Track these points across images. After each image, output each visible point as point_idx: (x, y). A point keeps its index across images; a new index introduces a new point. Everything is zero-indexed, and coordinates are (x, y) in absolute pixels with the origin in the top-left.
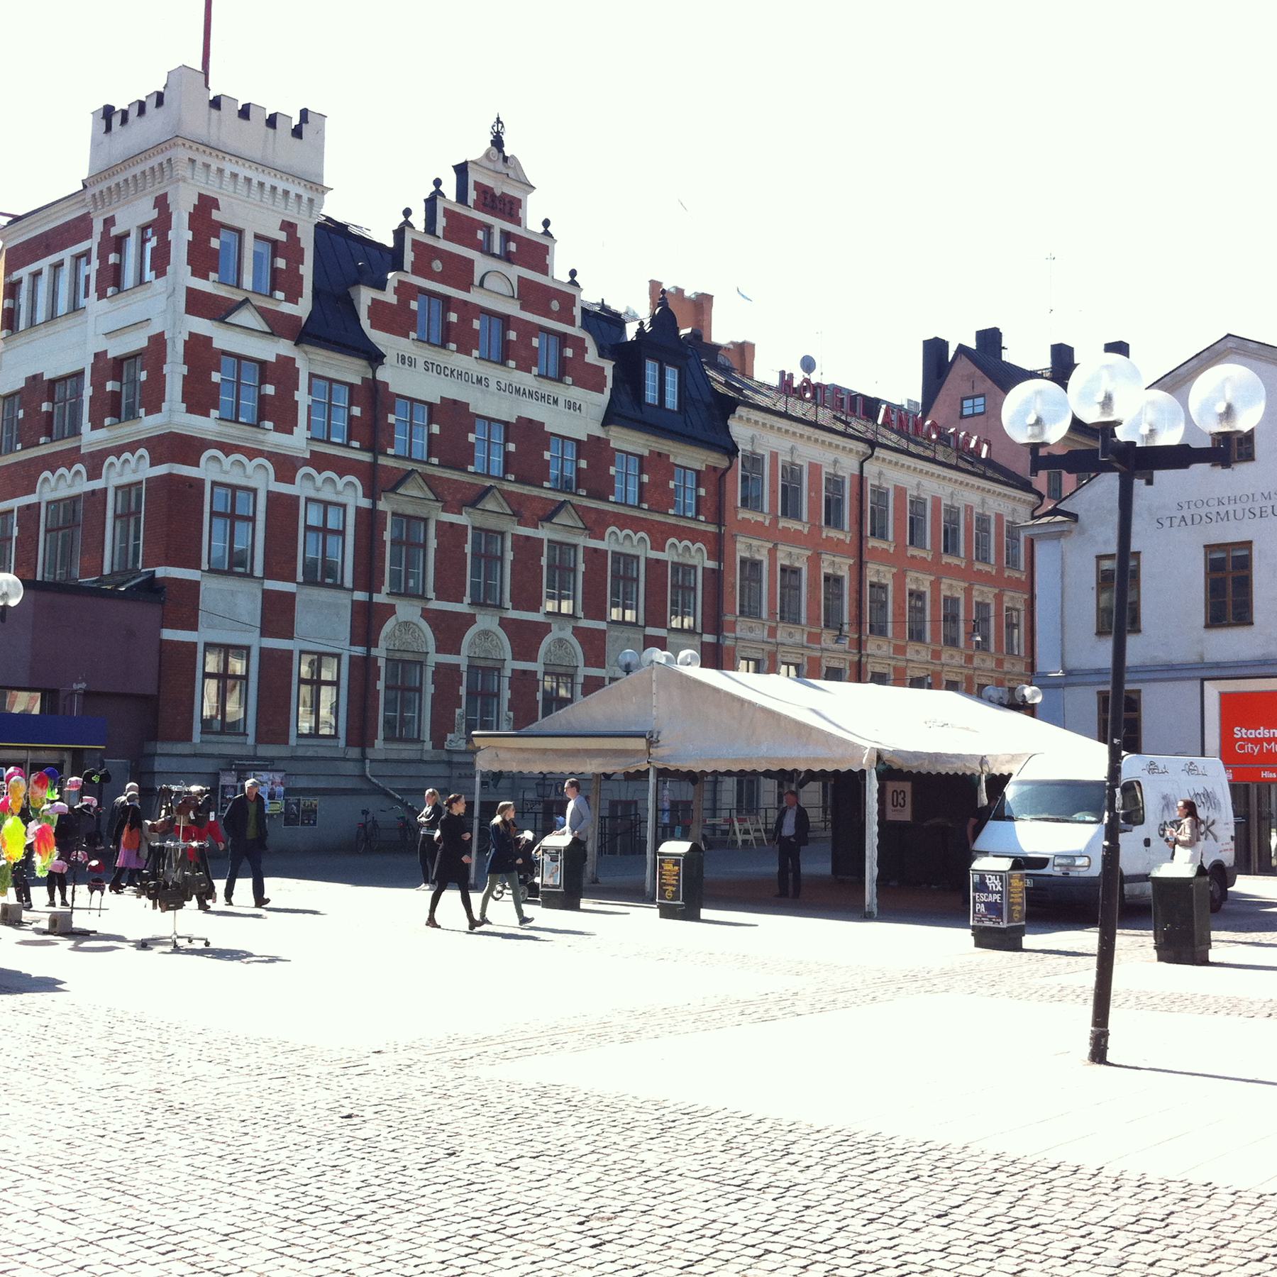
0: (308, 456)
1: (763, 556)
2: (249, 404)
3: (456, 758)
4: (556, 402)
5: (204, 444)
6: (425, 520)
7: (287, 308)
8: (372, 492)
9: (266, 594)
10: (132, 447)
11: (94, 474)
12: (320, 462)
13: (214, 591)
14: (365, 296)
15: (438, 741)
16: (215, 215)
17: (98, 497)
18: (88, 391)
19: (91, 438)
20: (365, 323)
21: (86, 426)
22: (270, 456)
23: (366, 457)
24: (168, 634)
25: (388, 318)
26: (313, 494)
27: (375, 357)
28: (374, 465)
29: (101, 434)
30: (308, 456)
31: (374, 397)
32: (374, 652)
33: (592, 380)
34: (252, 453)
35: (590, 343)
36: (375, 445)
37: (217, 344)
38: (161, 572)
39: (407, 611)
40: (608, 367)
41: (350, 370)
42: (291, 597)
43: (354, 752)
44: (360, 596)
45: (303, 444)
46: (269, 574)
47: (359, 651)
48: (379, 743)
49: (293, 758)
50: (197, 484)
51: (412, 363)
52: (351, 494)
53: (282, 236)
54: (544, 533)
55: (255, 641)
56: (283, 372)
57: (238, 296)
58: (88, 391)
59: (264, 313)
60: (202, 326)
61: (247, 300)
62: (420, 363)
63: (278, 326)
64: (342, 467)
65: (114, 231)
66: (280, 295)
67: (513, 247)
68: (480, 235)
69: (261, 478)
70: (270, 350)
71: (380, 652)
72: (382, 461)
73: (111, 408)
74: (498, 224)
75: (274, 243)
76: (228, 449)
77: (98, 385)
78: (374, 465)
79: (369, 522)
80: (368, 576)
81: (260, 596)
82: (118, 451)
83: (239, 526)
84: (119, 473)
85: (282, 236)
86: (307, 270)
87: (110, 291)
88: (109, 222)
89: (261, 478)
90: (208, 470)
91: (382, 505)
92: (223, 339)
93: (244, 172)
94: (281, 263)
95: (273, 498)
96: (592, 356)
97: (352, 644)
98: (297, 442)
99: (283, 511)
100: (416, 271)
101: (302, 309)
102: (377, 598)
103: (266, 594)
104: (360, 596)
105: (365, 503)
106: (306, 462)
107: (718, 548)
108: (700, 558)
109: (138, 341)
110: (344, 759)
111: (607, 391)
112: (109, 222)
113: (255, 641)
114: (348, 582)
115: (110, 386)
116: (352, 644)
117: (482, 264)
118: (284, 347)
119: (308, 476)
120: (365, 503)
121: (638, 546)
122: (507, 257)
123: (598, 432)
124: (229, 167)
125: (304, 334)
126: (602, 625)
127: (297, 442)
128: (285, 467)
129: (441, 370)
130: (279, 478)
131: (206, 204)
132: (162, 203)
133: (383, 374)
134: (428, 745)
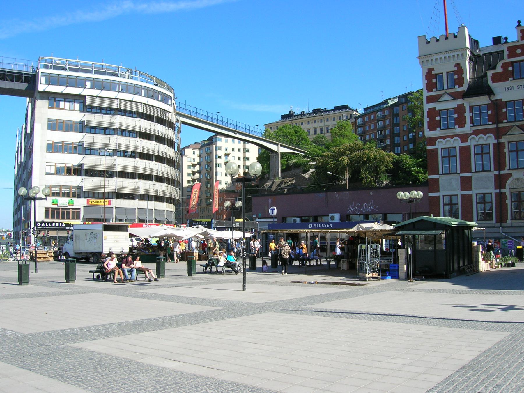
0: (472, 132)
7: (458, 89)
8: (498, 137)
9: (462, 178)
12: (476, 133)
13: (443, 180)
14: (490, 73)
16: (433, 72)
20: (490, 82)
22: (458, 136)
23: (494, 126)
25: (497, 78)
26: (476, 143)
27: (490, 92)
28: (498, 128)
30: (472, 132)
34: (452, 137)
36: (498, 121)
42: (471, 177)
44: (497, 172)
45: (469, 129)
46: (461, 172)
47: (498, 191)
48: (509, 221)
50: (436, 151)
51: (511, 88)
52: (491, 140)
53: (456, 69)
56: (460, 109)
57: (442, 92)
59: (450, 94)
60: (432, 105)
61: (446, 92)
62: (515, 87)
63: (455, 96)
64: (485, 132)
66: (457, 86)
70: (454, 104)
71: (506, 191)
72: (501, 125)
76: (444, 138)
78: (498, 128)
79: (499, 147)
80: (500, 164)
81: (459, 179)
83: (452, 159)
85: (456, 69)
89: (458, 143)
90: (439, 145)
91: (502, 141)
92: (438, 106)
94: (456, 77)
95: (461, 148)
97: (495, 189)
98: (467, 128)
99: (465, 151)
100: (509, 56)
101: (465, 88)
102: (502, 172)
104: (497, 172)
106: (471, 134)
113: (460, 193)
114: (492, 169)
116: (495, 189)
118: (460, 101)
119: (474, 138)
124: (434, 58)
127: (467, 128)
128: (464, 138)
133: (497, 97)
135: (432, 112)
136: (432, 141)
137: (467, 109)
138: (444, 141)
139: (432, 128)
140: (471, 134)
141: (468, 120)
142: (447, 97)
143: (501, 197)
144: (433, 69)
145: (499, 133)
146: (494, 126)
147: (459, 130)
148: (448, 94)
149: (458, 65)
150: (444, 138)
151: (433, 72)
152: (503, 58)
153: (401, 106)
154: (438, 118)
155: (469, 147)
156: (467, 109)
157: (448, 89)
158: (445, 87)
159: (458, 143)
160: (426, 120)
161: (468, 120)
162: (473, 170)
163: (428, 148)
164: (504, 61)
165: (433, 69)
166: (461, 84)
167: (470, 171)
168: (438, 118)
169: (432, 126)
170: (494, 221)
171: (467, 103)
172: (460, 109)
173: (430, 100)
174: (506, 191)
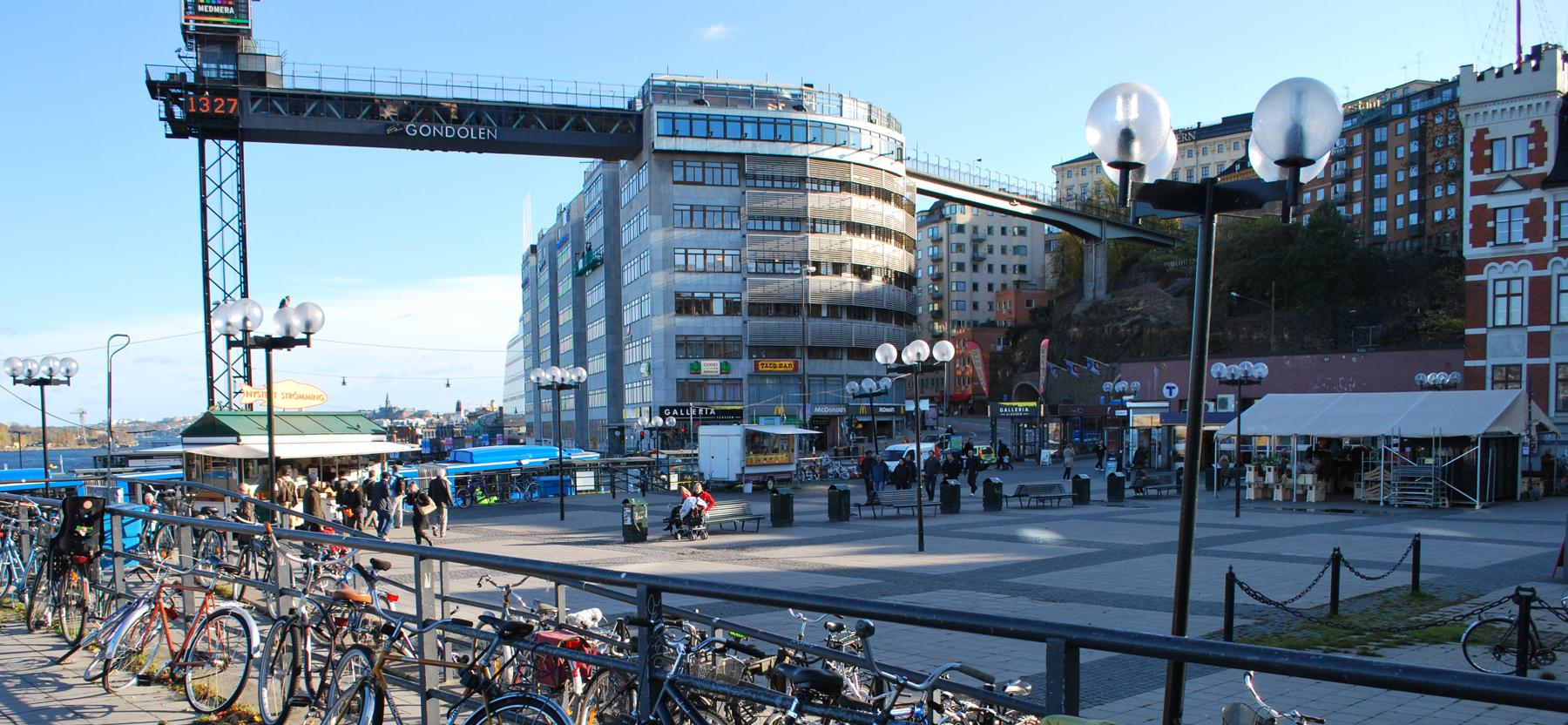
2: (1518, 234)
13: (1493, 338)
16: (1487, 137)
22: (1528, 257)
24: (1468, 363)
34: (1516, 259)
50: (1483, 284)
55: (1525, 361)
57: (1503, 176)
59: (1517, 180)
60: (1480, 200)
63: (1526, 183)
70: (1525, 199)
76: (1500, 260)
85: (1532, 131)
86: (1551, 145)
89: (1528, 271)
90: (1488, 275)
92: (1492, 202)
93: (1499, 107)
95: (1533, 281)
101: (1548, 167)
106: (1555, 255)
118: (1536, 193)
124: (1490, 109)
125: (1546, 182)
127: (1547, 244)
128: (1540, 261)
130: (1535, 268)
131: (1481, 133)
135: (1481, 213)
136: (1478, 266)
137: (1550, 208)
138: (1500, 267)
139: (1477, 242)
140: (1555, 255)
141: (1550, 228)
142: (1511, 185)
144: (1486, 131)
147: (1531, 247)
148: (1514, 179)
149: (1537, 124)
151: (1487, 137)
153: (1392, 124)
154: (1490, 224)
155: (1548, 279)
156: (1550, 208)
157: (1514, 169)
158: (1509, 167)
159: (1528, 271)
160: (1467, 226)
161: (1550, 228)
162: (1554, 321)
163: (1469, 278)
165: (1486, 131)
166: (1540, 163)
167: (1548, 323)
168: (1490, 224)
169: (1483, 236)
171: (1549, 198)
172: (1535, 211)
173: (1477, 189)
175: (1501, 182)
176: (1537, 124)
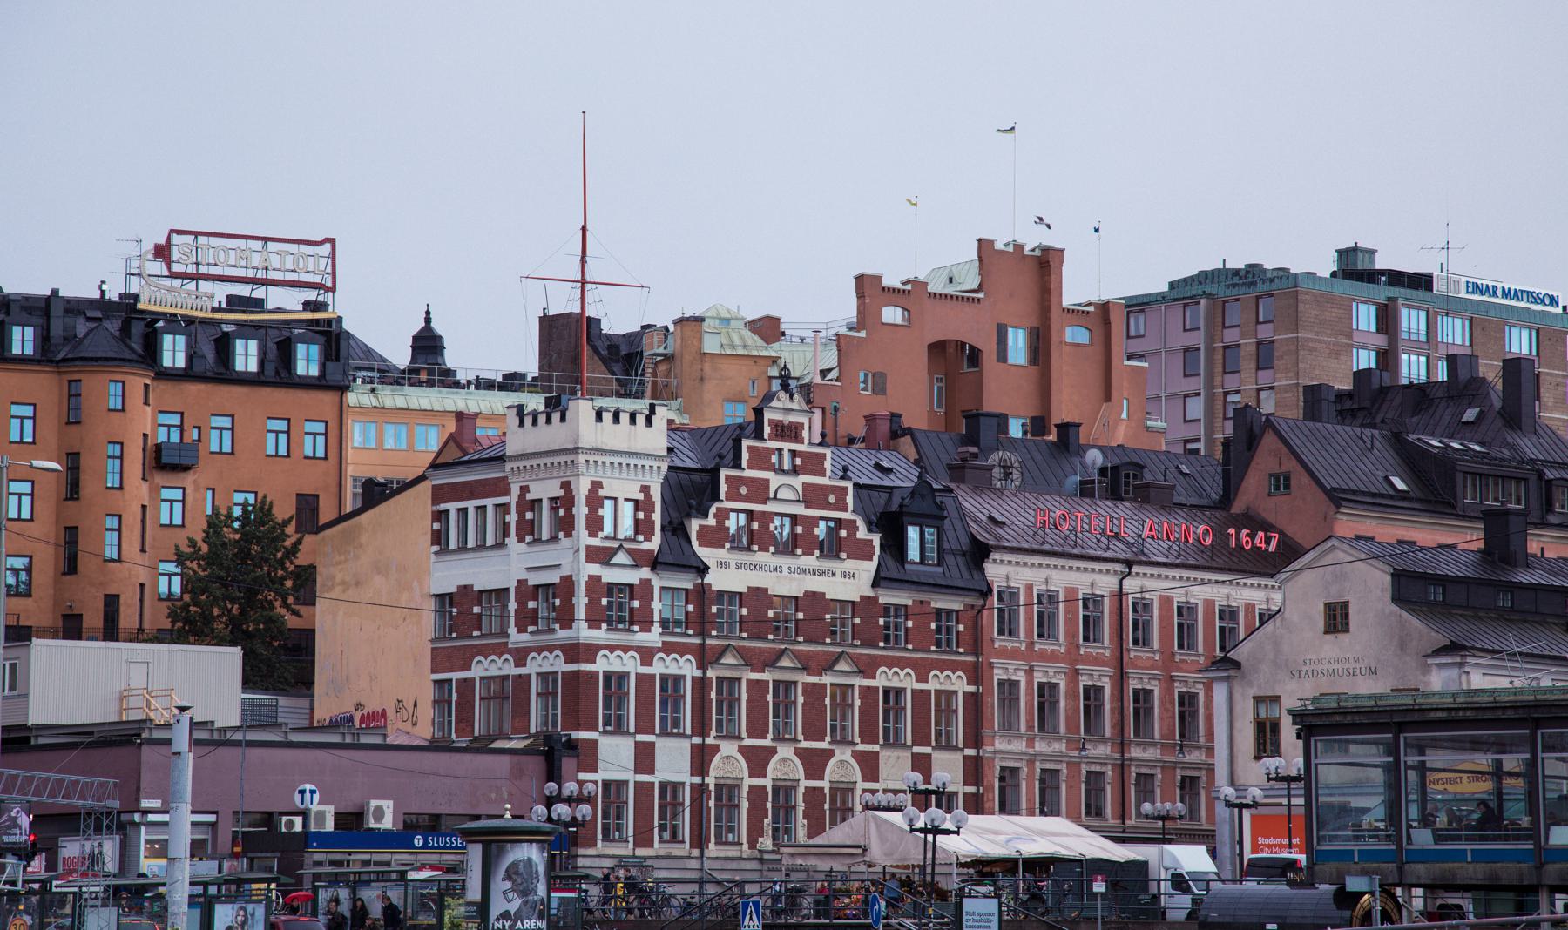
1: (1021, 677)
3: (766, 856)
4: (834, 574)
5: (599, 647)
6: (739, 680)
7: (646, 546)
8: (702, 665)
10: (551, 649)
11: (521, 662)
12: (668, 648)
14: (694, 525)
15: (752, 843)
17: (523, 681)
18: (512, 606)
19: (515, 638)
20: (695, 543)
21: (512, 630)
22: (638, 649)
27: (702, 570)
29: (525, 637)
31: (701, 594)
32: (707, 780)
33: (863, 552)
34: (626, 649)
35: (860, 523)
37: (605, 580)
38: (576, 735)
39: (729, 748)
40: (876, 539)
41: (686, 582)
43: (696, 853)
44: (697, 740)
47: (697, 780)
48: (712, 845)
49: (657, 857)
50: (594, 675)
51: (727, 565)
52: (687, 668)
53: (641, 497)
54: (827, 679)
55: (631, 777)
57: (616, 545)
58: (512, 606)
59: (630, 552)
60: (595, 569)
63: (639, 558)
64: (682, 650)
65: (529, 497)
67: (798, 461)
68: (774, 459)
69: (630, 665)
72: (708, 641)
73: (526, 619)
74: (787, 446)
75: (636, 502)
76: (612, 648)
77: (521, 603)
78: (703, 646)
79: (701, 684)
82: (540, 650)
84: (533, 667)
85: (641, 497)
86: (657, 517)
87: (528, 538)
88: (524, 490)
92: (609, 575)
93: (617, 460)
94: (641, 515)
95: (640, 678)
96: (862, 533)
98: (654, 637)
101: (654, 544)
103: (636, 743)
104: (697, 740)
105: (698, 673)
106: (659, 650)
107: (976, 674)
108: (959, 684)
109: (553, 578)
110: (689, 857)
111: (876, 558)
112: (524, 490)
115: (531, 604)
117: (775, 481)
118: (645, 573)
120: (698, 673)
121: (905, 680)
122: (795, 471)
123: (869, 592)
125: (656, 563)
126: (876, 748)
127: (654, 637)
128: (647, 655)
129: (747, 567)
131: (596, 485)
132: (566, 486)
134: (745, 846)
140: (659, 650)
143: (700, 791)
145: (705, 657)
146: (697, 641)
149: (645, 489)
150: (612, 648)
151: (602, 493)
152: (716, 498)
164: (717, 505)
170: (687, 845)
174: (710, 781)
175: (614, 552)
176: (645, 489)
